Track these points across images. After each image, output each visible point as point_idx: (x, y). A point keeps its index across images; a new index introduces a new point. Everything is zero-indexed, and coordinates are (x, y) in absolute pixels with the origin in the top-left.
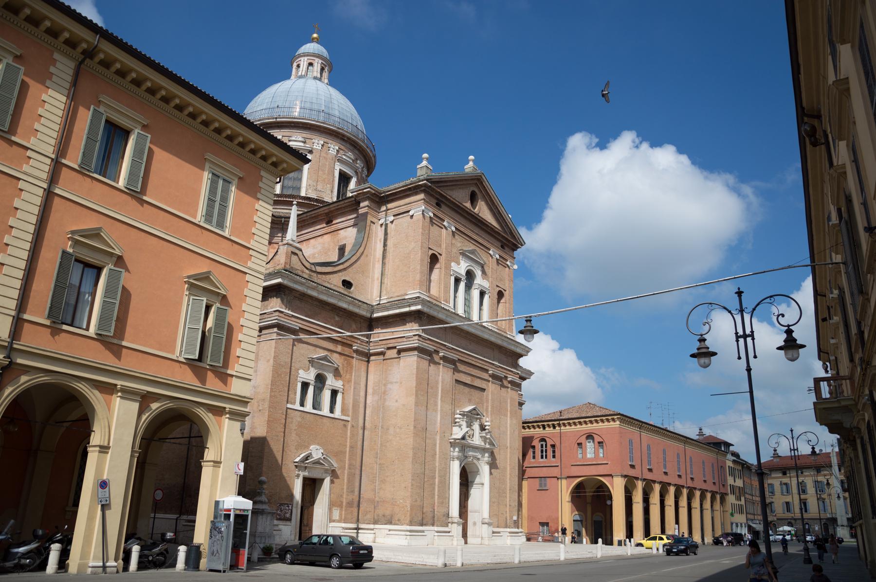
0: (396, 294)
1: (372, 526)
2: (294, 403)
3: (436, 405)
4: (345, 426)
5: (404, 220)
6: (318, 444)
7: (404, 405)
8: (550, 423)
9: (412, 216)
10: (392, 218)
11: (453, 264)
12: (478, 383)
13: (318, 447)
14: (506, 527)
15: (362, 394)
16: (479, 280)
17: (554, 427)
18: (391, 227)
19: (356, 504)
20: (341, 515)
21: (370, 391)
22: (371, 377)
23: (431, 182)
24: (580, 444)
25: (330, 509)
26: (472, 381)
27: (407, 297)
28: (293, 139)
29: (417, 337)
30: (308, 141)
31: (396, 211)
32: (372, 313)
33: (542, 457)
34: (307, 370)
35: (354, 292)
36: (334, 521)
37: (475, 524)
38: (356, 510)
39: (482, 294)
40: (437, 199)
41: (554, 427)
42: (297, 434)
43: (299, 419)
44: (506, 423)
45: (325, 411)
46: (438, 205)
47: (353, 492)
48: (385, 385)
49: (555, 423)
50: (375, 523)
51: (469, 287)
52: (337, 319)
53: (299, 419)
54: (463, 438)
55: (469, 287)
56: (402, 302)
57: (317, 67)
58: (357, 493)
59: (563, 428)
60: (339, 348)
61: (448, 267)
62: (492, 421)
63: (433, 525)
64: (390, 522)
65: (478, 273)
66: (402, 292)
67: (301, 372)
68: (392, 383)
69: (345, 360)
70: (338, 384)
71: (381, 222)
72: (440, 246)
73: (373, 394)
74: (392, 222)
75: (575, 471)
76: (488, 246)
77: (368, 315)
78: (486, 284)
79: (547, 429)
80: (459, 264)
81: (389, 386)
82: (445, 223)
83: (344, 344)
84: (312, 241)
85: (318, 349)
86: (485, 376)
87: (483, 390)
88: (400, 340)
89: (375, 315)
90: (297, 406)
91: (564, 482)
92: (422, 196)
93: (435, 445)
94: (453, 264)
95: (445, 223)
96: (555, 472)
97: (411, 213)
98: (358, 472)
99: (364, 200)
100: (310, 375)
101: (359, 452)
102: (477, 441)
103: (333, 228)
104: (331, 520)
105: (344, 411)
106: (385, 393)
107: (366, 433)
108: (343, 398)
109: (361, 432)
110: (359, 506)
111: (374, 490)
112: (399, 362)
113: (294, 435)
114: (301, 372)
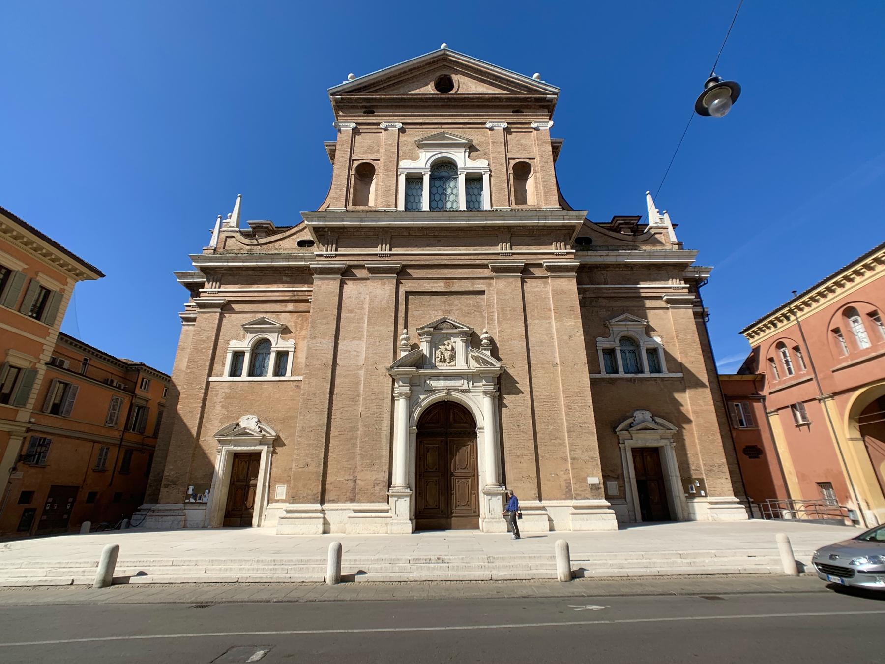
8: (778, 314)
12: (479, 286)
17: (788, 318)
24: (836, 331)
40: (362, 107)
41: (788, 318)
42: (222, 407)
44: (549, 329)
49: (785, 311)
59: (799, 314)
60: (290, 307)
63: (352, 500)
72: (378, 152)
75: (843, 380)
79: (779, 325)
87: (482, 293)
91: (830, 403)
93: (358, 383)
96: (810, 390)
100: (245, 344)
113: (218, 408)
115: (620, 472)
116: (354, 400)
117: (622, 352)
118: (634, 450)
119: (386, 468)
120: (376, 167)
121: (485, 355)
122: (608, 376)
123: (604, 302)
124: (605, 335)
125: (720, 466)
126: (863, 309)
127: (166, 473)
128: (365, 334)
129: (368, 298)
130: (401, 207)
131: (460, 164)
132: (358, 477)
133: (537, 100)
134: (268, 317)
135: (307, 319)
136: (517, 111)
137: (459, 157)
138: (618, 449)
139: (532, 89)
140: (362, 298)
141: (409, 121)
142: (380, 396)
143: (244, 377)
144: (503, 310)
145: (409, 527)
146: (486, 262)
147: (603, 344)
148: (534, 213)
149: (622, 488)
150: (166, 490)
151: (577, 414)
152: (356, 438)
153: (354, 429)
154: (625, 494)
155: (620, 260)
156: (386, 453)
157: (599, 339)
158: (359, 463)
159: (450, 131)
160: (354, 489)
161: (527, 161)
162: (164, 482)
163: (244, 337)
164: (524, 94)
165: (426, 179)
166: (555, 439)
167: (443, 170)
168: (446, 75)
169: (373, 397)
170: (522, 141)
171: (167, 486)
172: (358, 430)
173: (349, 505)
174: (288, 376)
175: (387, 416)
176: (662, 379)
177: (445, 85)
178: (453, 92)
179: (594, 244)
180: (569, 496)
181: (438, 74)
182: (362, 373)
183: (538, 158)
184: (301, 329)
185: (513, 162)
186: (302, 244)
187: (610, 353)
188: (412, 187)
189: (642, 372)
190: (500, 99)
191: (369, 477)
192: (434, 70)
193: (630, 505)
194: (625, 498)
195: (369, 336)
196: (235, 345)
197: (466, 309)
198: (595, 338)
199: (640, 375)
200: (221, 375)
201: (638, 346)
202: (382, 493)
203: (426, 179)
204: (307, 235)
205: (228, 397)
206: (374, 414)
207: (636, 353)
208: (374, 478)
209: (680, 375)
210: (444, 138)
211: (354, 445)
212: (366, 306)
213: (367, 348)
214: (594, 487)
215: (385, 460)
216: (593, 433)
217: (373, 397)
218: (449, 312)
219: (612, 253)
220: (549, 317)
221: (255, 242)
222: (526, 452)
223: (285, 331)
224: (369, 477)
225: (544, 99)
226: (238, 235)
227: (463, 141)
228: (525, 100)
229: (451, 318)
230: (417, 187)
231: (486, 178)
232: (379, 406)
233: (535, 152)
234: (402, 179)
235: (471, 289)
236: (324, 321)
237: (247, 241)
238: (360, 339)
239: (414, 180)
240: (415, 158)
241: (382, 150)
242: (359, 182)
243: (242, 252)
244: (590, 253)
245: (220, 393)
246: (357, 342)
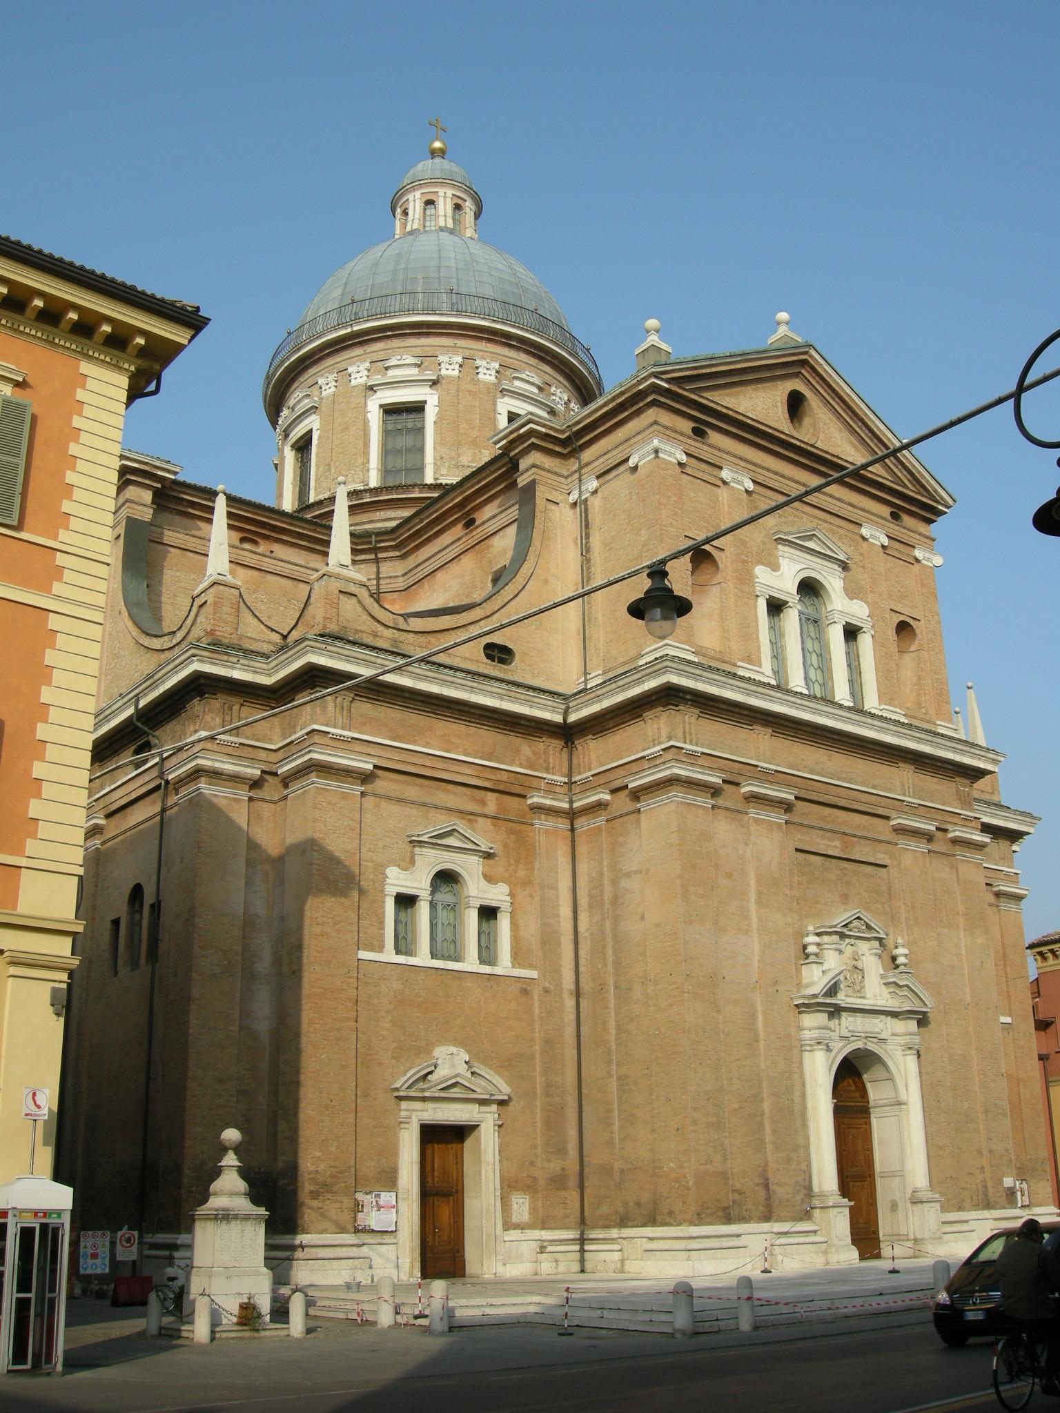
0: (621, 660)
1: (614, 1233)
2: (380, 948)
3: (746, 917)
4: (525, 992)
5: (620, 482)
6: (457, 1042)
7: (658, 925)
9: (636, 468)
10: (593, 484)
11: (760, 571)
13: (453, 1049)
14: (988, 1206)
15: (565, 911)
16: (841, 605)
18: (596, 503)
19: (573, 1181)
20: (533, 1210)
21: (583, 901)
22: (582, 867)
23: (668, 381)
25: (505, 1201)
26: (846, 847)
27: (641, 662)
28: (393, 362)
29: (669, 755)
30: (427, 361)
31: (601, 465)
32: (566, 713)
34: (409, 863)
35: (517, 670)
36: (517, 1226)
37: (894, 1207)
38: (574, 1196)
39: (851, 633)
43: (397, 986)
45: (471, 963)
46: (699, 433)
47: (562, 1151)
48: (614, 882)
50: (607, 1227)
51: (813, 623)
53: (397, 986)
54: (833, 990)
55: (813, 623)
56: (632, 672)
57: (444, 207)
58: (573, 1152)
61: (746, 578)
62: (910, 945)
63: (767, 1218)
64: (652, 1221)
65: (833, 582)
66: (633, 653)
67: (392, 872)
68: (628, 875)
69: (510, 832)
70: (497, 895)
71: (574, 496)
73: (591, 907)
74: (595, 492)
76: (854, 514)
77: (559, 719)
78: (858, 611)
80: (775, 567)
81: (624, 883)
82: (725, 474)
84: (439, 575)
85: (433, 814)
86: (881, 829)
88: (635, 767)
89: (572, 718)
90: (389, 955)
92: (651, 414)
93: (753, 1017)
94: (760, 571)
95: (725, 474)
97: (631, 463)
98: (572, 1102)
99: (526, 452)
100: (418, 882)
101: (571, 1053)
102: (876, 993)
103: (478, 534)
104: (508, 1225)
105: (518, 956)
106: (615, 900)
107: (583, 1003)
108: (514, 925)
109: (570, 1003)
110: (581, 1186)
111: (610, 1143)
112: (638, 821)
114: (392, 872)
140: (741, 852)
143: (422, 958)
150: (315, 1203)
153: (757, 1098)
160: (768, 1198)
171: (315, 1195)
173: (765, 1226)
174: (504, 965)
182: (758, 998)
196: (397, 880)
197: (865, 894)
200: (380, 948)
220: (958, 928)
229: (867, 917)
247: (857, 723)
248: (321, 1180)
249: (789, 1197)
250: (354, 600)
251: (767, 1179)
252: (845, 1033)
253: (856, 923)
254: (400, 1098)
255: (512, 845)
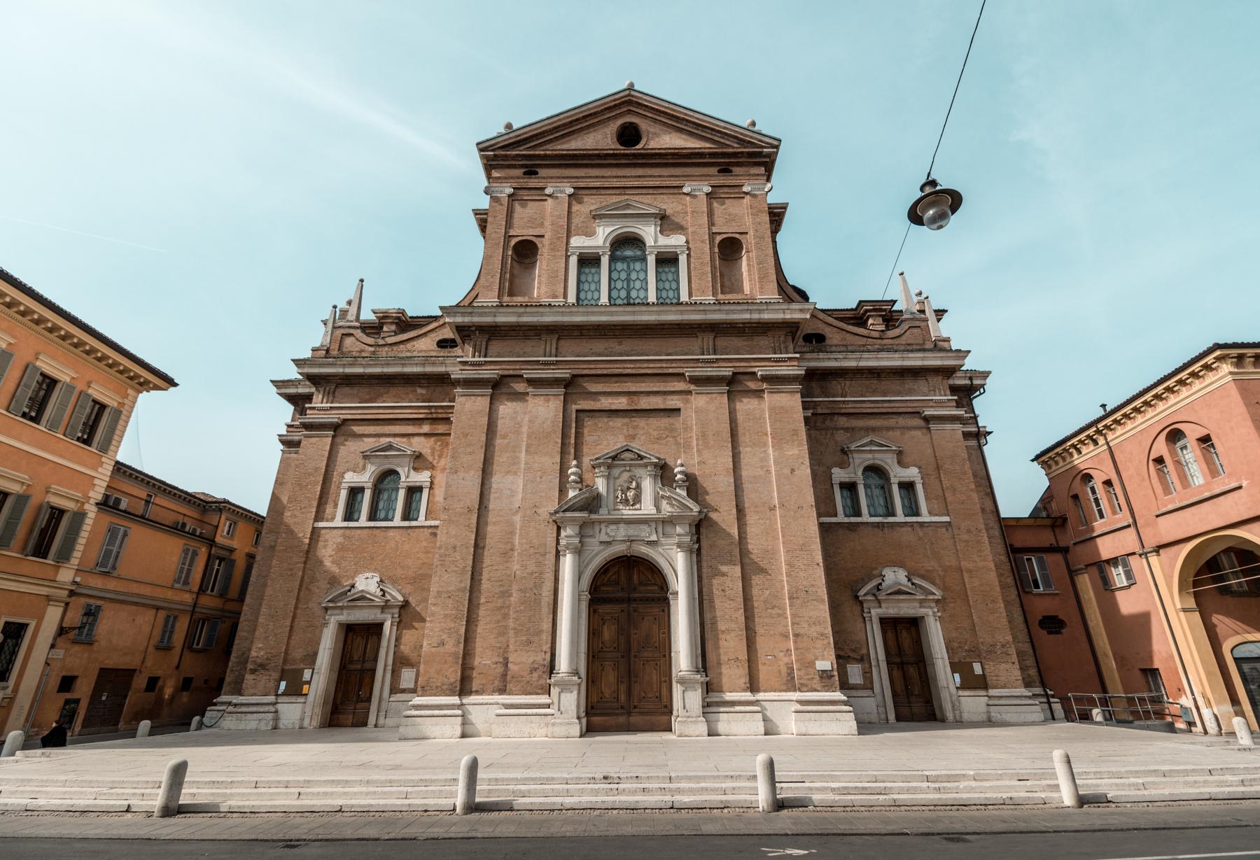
2: (333, 519)
8: (1082, 436)
12: (673, 402)
13: (369, 575)
17: (1095, 442)
33: (1114, 513)
36: (403, 691)
40: (522, 166)
41: (1095, 442)
43: (340, 540)
44: (765, 459)
49: (1091, 431)
52: (419, 391)
53: (340, 540)
59: (1110, 436)
60: (426, 428)
63: (502, 691)
70: (422, 478)
72: (542, 225)
75: (1170, 528)
78: (675, 241)
79: (1084, 450)
80: (590, 234)
83: (434, 421)
93: (512, 533)
100: (365, 477)
115: (864, 651)
116: (507, 555)
117: (866, 486)
118: (886, 622)
119: (547, 647)
120: (539, 246)
121: (679, 495)
122: (846, 520)
123: (843, 421)
124: (843, 465)
125: (1003, 646)
126: (1192, 433)
127: (253, 654)
128: (523, 466)
129: (527, 419)
130: (572, 298)
131: (650, 242)
132: (511, 659)
133: (751, 155)
134: (396, 441)
135: (447, 444)
136: (725, 170)
137: (649, 233)
138: (861, 620)
139: (744, 141)
141: (582, 185)
142: (542, 550)
143: (363, 521)
144: (704, 435)
145: (576, 730)
146: (680, 371)
147: (839, 475)
148: (745, 307)
149: (867, 674)
150: (253, 676)
151: (802, 574)
152: (509, 607)
154: (872, 683)
155: (863, 364)
156: (547, 626)
157: (835, 471)
158: (512, 641)
159: (636, 198)
160: (504, 675)
161: (737, 236)
162: (250, 666)
163: (364, 468)
164: (736, 148)
165: (605, 261)
166: (773, 607)
167: (626, 243)
168: (631, 124)
169: (532, 551)
170: (731, 210)
171: (253, 671)
172: (511, 595)
174: (421, 520)
175: (549, 576)
176: (921, 524)
177: (629, 135)
178: (640, 146)
179: (828, 342)
180: (791, 685)
181: (620, 122)
183: (751, 233)
184: (440, 456)
185: (719, 238)
186: (443, 344)
187: (850, 487)
188: (587, 270)
189: (894, 515)
190: (701, 155)
191: (521, 660)
192: (615, 117)
193: (880, 697)
194: (872, 688)
195: (528, 468)
196: (351, 478)
197: (655, 433)
198: (830, 468)
199: (891, 519)
201: (888, 479)
202: (542, 682)
203: (605, 261)
204: (448, 334)
205: (341, 548)
206: (532, 573)
207: (885, 488)
208: (531, 660)
209: (947, 519)
210: (628, 206)
211: (506, 616)
212: (525, 429)
213: (525, 485)
214: (825, 675)
215: (546, 637)
216: (823, 600)
217: (532, 551)
218: (633, 437)
219: (850, 355)
220: (765, 444)
221: (381, 342)
222: (733, 626)
223: (418, 461)
224: (521, 660)
225: (760, 154)
226: (358, 333)
227: (653, 211)
228: (735, 155)
229: (635, 445)
230: (593, 270)
231: (683, 259)
232: (539, 564)
233: (748, 223)
234: (573, 261)
235: (662, 407)
236: (469, 450)
237: (370, 340)
238: (516, 473)
239: (588, 261)
240: (590, 234)
241: (547, 224)
242: (515, 264)
243: (364, 354)
244: (822, 355)
245: (330, 543)
246: (510, 478)
247: (634, 313)
248: (259, 661)
249: (525, 674)
250: (352, 338)
251: (506, 659)
252: (604, 538)
253: (627, 455)
254: (326, 609)
255: (437, 448)
